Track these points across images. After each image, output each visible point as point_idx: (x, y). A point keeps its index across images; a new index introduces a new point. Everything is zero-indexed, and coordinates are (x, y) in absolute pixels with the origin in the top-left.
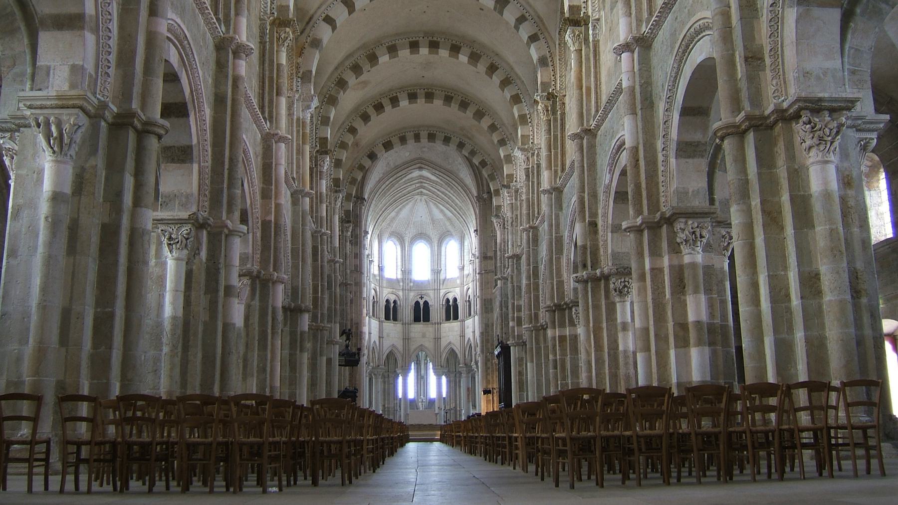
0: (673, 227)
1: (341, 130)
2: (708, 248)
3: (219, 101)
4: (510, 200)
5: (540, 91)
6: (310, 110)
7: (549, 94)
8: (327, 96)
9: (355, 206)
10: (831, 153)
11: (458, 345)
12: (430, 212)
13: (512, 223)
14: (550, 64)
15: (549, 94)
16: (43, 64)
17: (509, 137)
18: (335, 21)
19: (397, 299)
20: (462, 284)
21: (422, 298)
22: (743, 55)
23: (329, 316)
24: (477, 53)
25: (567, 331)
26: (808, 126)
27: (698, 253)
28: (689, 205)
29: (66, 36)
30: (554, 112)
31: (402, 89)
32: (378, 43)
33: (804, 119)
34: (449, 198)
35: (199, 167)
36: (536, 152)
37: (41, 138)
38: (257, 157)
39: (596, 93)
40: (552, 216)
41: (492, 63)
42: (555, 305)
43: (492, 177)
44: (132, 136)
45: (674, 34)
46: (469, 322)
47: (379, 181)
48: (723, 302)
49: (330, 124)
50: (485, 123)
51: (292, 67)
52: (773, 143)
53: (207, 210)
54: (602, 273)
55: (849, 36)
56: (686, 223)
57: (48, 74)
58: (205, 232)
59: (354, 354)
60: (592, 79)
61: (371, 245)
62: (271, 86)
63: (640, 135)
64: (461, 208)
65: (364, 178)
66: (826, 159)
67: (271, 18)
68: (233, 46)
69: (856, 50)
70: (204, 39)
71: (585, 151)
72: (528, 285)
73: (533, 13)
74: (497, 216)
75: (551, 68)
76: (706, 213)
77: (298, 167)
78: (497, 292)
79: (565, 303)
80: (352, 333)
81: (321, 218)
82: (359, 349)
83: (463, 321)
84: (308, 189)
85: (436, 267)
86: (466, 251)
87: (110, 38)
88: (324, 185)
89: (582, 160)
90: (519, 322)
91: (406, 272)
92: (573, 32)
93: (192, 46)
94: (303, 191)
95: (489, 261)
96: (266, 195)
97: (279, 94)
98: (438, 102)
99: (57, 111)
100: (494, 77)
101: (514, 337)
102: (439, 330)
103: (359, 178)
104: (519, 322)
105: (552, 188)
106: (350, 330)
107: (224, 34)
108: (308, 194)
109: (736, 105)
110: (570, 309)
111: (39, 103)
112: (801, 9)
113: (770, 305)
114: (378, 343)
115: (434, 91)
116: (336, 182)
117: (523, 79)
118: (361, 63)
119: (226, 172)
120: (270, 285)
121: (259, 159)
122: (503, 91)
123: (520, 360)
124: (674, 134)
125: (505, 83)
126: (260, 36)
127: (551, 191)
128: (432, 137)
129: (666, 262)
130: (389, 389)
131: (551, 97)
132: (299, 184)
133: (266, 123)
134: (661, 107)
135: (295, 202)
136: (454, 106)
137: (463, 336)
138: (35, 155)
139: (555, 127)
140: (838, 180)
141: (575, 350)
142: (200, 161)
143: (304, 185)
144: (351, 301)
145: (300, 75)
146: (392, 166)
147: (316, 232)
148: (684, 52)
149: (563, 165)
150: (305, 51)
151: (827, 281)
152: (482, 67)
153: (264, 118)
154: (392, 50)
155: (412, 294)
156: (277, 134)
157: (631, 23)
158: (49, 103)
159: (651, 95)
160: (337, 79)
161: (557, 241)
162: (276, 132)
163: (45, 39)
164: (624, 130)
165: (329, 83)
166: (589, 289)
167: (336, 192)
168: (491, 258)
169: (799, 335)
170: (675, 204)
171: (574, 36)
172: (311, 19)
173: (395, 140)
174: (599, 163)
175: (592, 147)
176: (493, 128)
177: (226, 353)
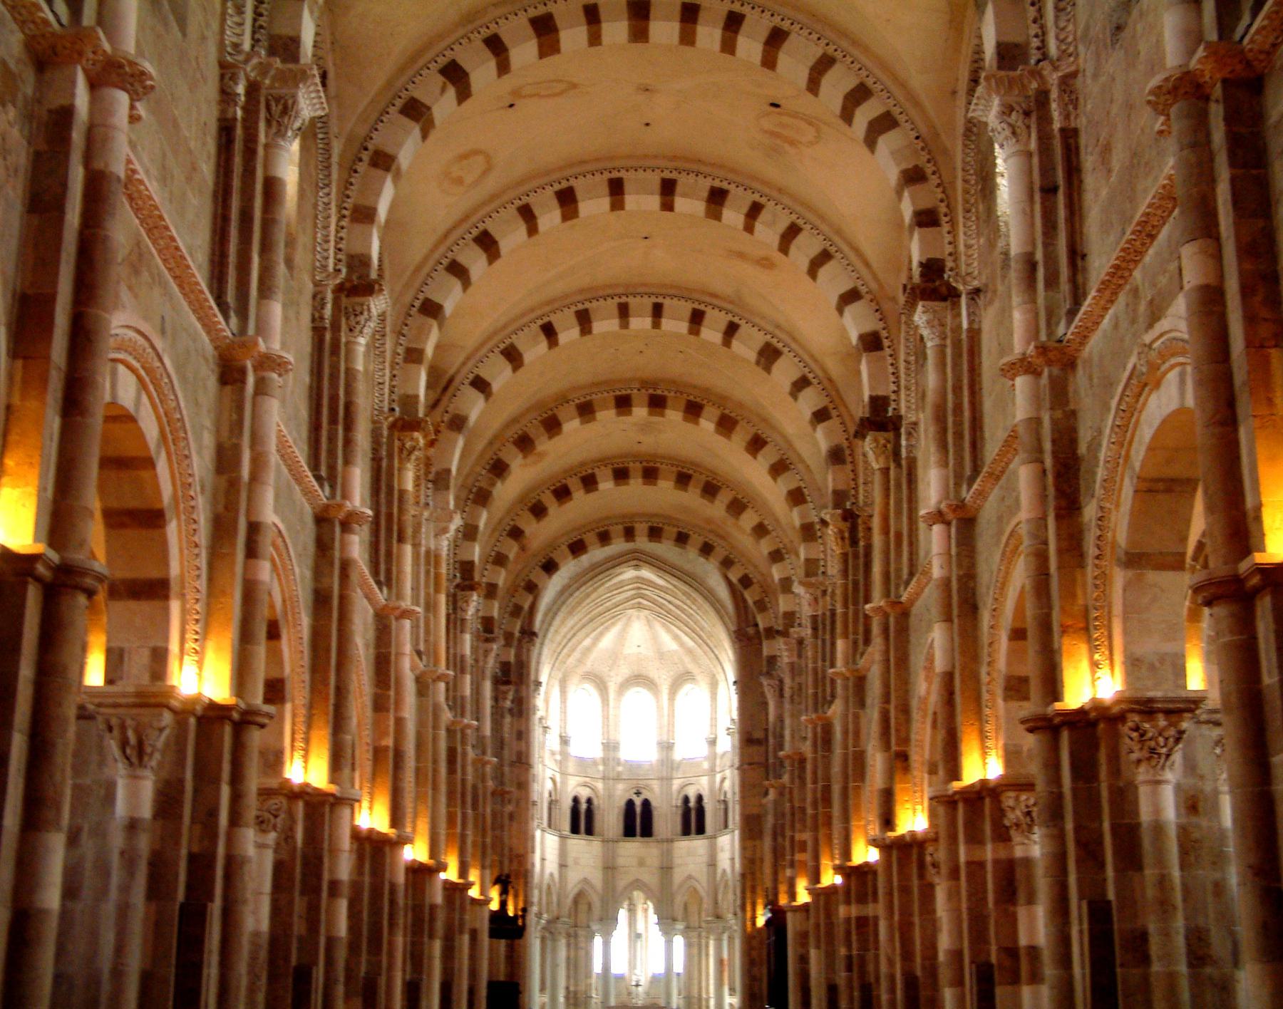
0: (999, 802)
1: (497, 534)
3: (321, 600)
4: (788, 656)
6: (448, 535)
8: (474, 490)
9: (519, 648)
11: (705, 884)
12: (655, 638)
13: (792, 697)
14: (849, 459)
17: (789, 545)
19: (593, 796)
20: (712, 771)
21: (638, 793)
24: (730, 417)
25: (870, 910)
26: (1135, 735)
27: (1035, 842)
28: (1022, 771)
30: (854, 542)
31: (603, 461)
32: (563, 399)
33: (1130, 724)
36: (830, 590)
37: (113, 746)
39: (911, 544)
44: (228, 730)
45: (1000, 519)
49: (479, 536)
50: (749, 520)
51: (418, 465)
56: (1017, 799)
60: (905, 519)
61: (547, 701)
62: (389, 530)
63: (957, 656)
66: (1159, 778)
67: (391, 419)
68: (341, 515)
71: (892, 635)
72: (815, 817)
73: (820, 373)
74: (769, 674)
75: (849, 467)
77: (427, 632)
81: (463, 698)
83: (714, 837)
88: (467, 637)
89: (887, 652)
91: (610, 747)
92: (876, 440)
93: (288, 541)
94: (435, 671)
95: (755, 749)
96: (380, 705)
97: (401, 539)
99: (134, 711)
103: (526, 606)
107: (327, 499)
111: (110, 701)
112: (1130, 573)
114: (556, 875)
115: (658, 465)
116: (488, 624)
117: (809, 462)
118: (532, 433)
120: (387, 849)
121: (372, 651)
123: (803, 937)
125: (778, 469)
126: (373, 449)
127: (848, 674)
128: (655, 533)
130: (576, 957)
131: (850, 517)
132: (428, 661)
133: (381, 590)
137: (712, 864)
138: (102, 764)
139: (856, 567)
143: (436, 662)
144: (511, 817)
145: (431, 477)
147: (453, 723)
150: (441, 437)
152: (740, 438)
153: (379, 583)
156: (398, 608)
157: (946, 479)
158: (123, 701)
159: (974, 594)
160: (491, 462)
162: (397, 604)
165: (478, 469)
167: (487, 640)
168: (758, 742)
171: (877, 447)
172: (451, 381)
173: (590, 538)
174: (912, 658)
175: (903, 630)
176: (760, 530)
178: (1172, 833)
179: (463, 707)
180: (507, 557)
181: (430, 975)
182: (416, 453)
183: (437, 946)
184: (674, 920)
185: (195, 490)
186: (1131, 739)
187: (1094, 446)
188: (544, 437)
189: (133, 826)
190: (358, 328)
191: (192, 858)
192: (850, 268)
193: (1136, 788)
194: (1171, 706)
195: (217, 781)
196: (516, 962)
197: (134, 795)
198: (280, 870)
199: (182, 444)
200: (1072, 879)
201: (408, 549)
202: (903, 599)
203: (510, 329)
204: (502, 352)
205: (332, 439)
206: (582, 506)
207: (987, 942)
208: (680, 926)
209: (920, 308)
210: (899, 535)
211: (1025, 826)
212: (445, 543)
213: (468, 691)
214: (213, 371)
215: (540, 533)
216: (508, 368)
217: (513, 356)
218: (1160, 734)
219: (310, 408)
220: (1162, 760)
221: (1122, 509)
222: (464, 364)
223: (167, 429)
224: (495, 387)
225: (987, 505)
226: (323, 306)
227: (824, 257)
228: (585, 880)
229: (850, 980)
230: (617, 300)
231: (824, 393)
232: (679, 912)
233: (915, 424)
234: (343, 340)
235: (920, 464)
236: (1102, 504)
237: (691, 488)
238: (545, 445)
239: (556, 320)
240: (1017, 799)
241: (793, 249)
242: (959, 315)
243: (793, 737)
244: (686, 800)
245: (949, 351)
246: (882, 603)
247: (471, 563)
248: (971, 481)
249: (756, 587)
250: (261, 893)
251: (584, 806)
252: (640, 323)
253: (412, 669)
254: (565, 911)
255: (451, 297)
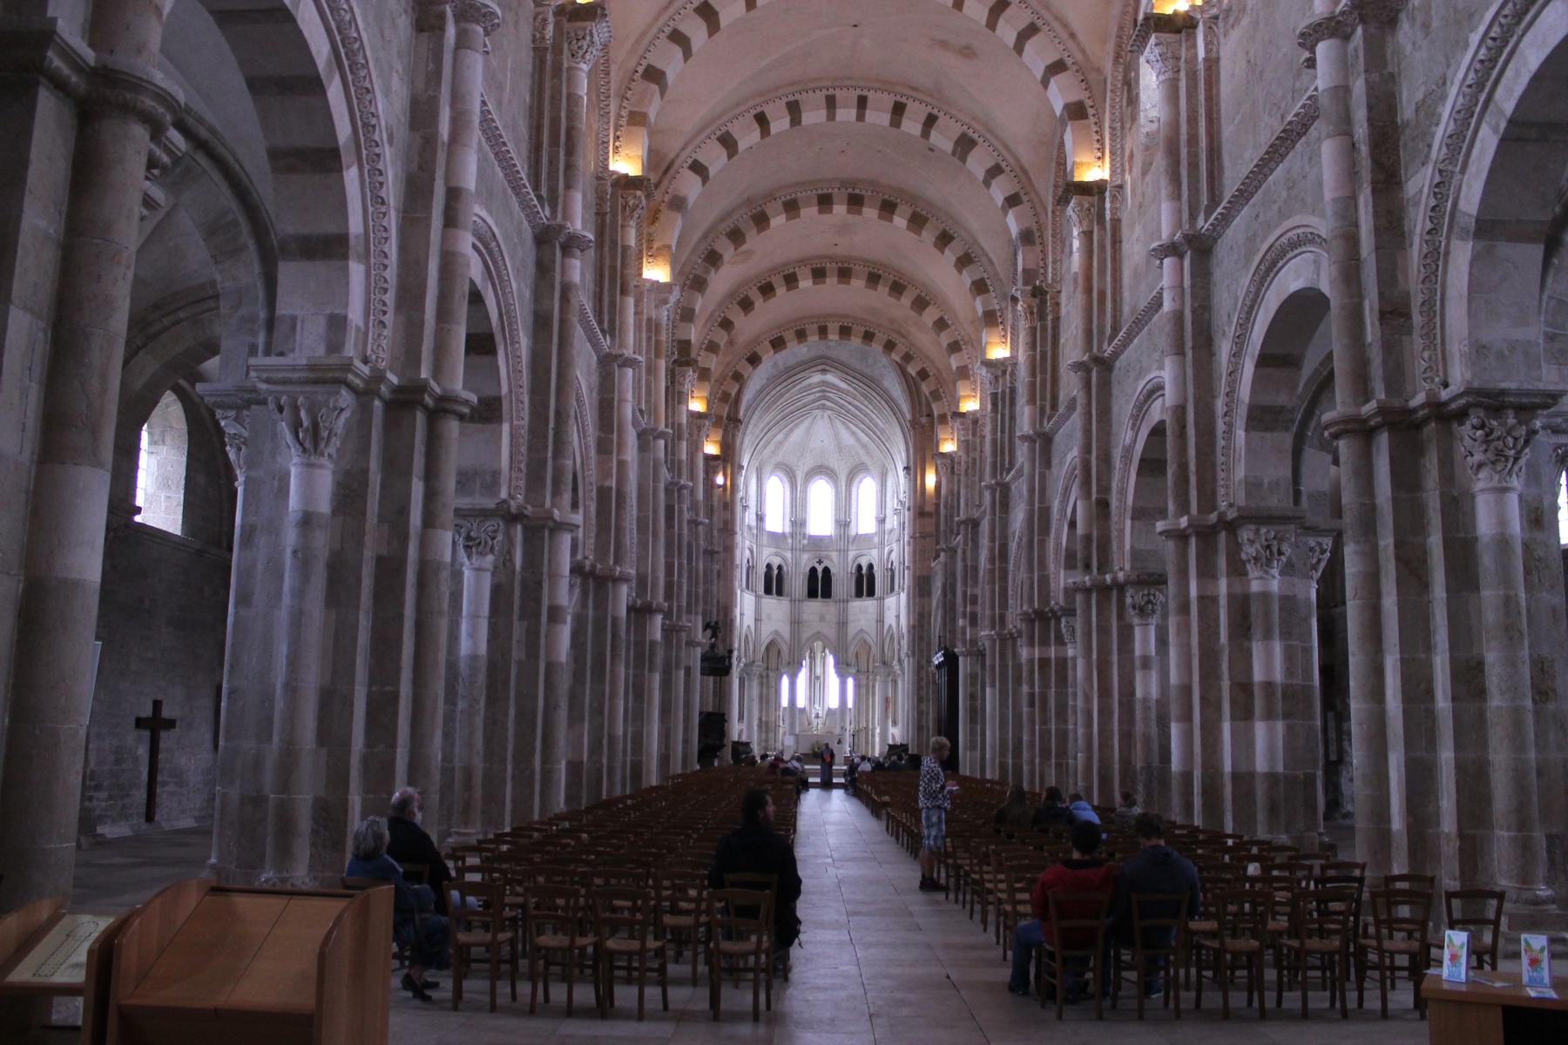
0: (1236, 536)
2: (1288, 570)
3: (541, 323)
5: (1020, 283)
7: (1035, 288)
10: (1514, 476)
11: (873, 634)
12: (836, 435)
13: (966, 470)
14: (1038, 241)
15: (1035, 288)
16: (283, 312)
17: (966, 338)
18: (706, 169)
21: (820, 562)
22: (1376, 306)
23: (689, 604)
25: (1052, 652)
26: (1479, 433)
28: (1262, 504)
29: (319, 269)
30: (1042, 317)
31: (802, 262)
32: (770, 196)
33: (1475, 421)
34: (866, 415)
35: (511, 428)
38: (591, 391)
39: (1114, 301)
40: (1034, 476)
41: (944, 230)
42: (1035, 612)
43: (936, 395)
44: (420, 418)
45: (1251, 240)
46: (890, 601)
47: (760, 391)
48: (1307, 651)
50: (930, 315)
52: (1418, 450)
53: (523, 491)
54: (1114, 579)
55: (1549, 280)
56: (1257, 531)
57: (293, 328)
58: (519, 530)
59: (723, 658)
64: (882, 431)
65: (739, 392)
66: (1504, 484)
68: (562, 238)
69: (1559, 301)
70: (519, 232)
73: (1012, 161)
75: (1038, 248)
76: (1289, 518)
77: (649, 393)
78: (937, 566)
79: (1052, 611)
80: (720, 626)
81: (680, 462)
82: (731, 652)
83: (882, 599)
84: (662, 426)
85: (842, 517)
86: (889, 494)
87: (386, 267)
89: (1089, 404)
90: (973, 620)
91: (798, 523)
92: (1080, 204)
93: (503, 247)
94: (654, 430)
95: (927, 520)
96: (604, 448)
97: (624, 292)
98: (858, 283)
99: (308, 388)
100: (947, 251)
101: (964, 642)
102: (845, 611)
103: (733, 394)
104: (973, 620)
105: (1035, 433)
106: (717, 623)
108: (662, 435)
109: (1362, 390)
110: (1058, 620)
111: (280, 375)
112: (1481, 245)
113: (1401, 705)
114: (753, 627)
117: (992, 256)
118: (742, 226)
119: (551, 433)
120: (610, 584)
121: (595, 394)
122: (960, 272)
123: (973, 677)
124: (1245, 392)
125: (964, 261)
129: (1223, 586)
130: (768, 694)
131: (1038, 293)
132: (649, 418)
134: (1224, 349)
135: (644, 446)
136: (883, 290)
137: (880, 620)
139: (1044, 339)
140: (1521, 516)
141: (1062, 679)
142: (512, 418)
143: (657, 420)
146: (782, 367)
147: (671, 483)
148: (1269, 270)
149: (1055, 398)
150: (662, 216)
151: (1494, 676)
152: (928, 235)
153: (603, 331)
154: (791, 208)
155: (805, 557)
157: (1180, 211)
158: (296, 375)
161: (1041, 515)
163: (287, 272)
164: (1161, 368)
166: (1094, 602)
168: (929, 515)
169: (1446, 756)
170: (1241, 500)
171: (1081, 210)
173: (789, 335)
174: (1115, 409)
176: (941, 324)
177: (550, 708)
178: (1519, 549)
179: (680, 469)
180: (719, 346)
181: (650, 704)
182: (639, 211)
183: (657, 677)
184: (848, 665)
185: (381, 135)
186: (1475, 440)
187: (1428, 108)
188: (754, 231)
189: (307, 521)
190: (581, 53)
191: (380, 561)
192: (1057, 41)
193: (1473, 496)
194: (1524, 400)
195: (408, 473)
196: (722, 694)
197: (308, 487)
198: (499, 594)
199: (363, 73)
200: (1390, 602)
201: (631, 301)
202: (1106, 355)
203: (725, 118)
204: (718, 139)
205: (553, 161)
206: (784, 305)
207: (1218, 678)
208: (853, 670)
209: (1153, 40)
210: (1102, 295)
211: (1264, 560)
212: (666, 313)
213: (684, 457)
214: (406, 12)
215: (749, 327)
216: (724, 154)
217: (728, 142)
218: (1509, 433)
219: (531, 128)
220: (1509, 465)
221: (1472, 169)
222: (683, 149)
223: (342, 51)
224: (712, 172)
225: (1229, 232)
226: (544, 27)
227: (1030, 31)
228: (776, 632)
229: (1032, 715)
230: (825, 92)
231: (1016, 180)
232: (853, 661)
233: (1121, 187)
234: (565, 65)
235: (1124, 224)
236: (1441, 166)
237: (880, 287)
238: (753, 240)
239: (769, 111)
240: (1257, 531)
241: (1001, 23)
242: (1195, 46)
243: (967, 505)
244: (859, 567)
245: (1183, 84)
246: (1085, 358)
247: (688, 342)
248: (1209, 211)
249: (931, 379)
250: (478, 617)
251: (776, 572)
252: (846, 114)
253: (635, 423)
254: (759, 656)
255: (671, 62)
